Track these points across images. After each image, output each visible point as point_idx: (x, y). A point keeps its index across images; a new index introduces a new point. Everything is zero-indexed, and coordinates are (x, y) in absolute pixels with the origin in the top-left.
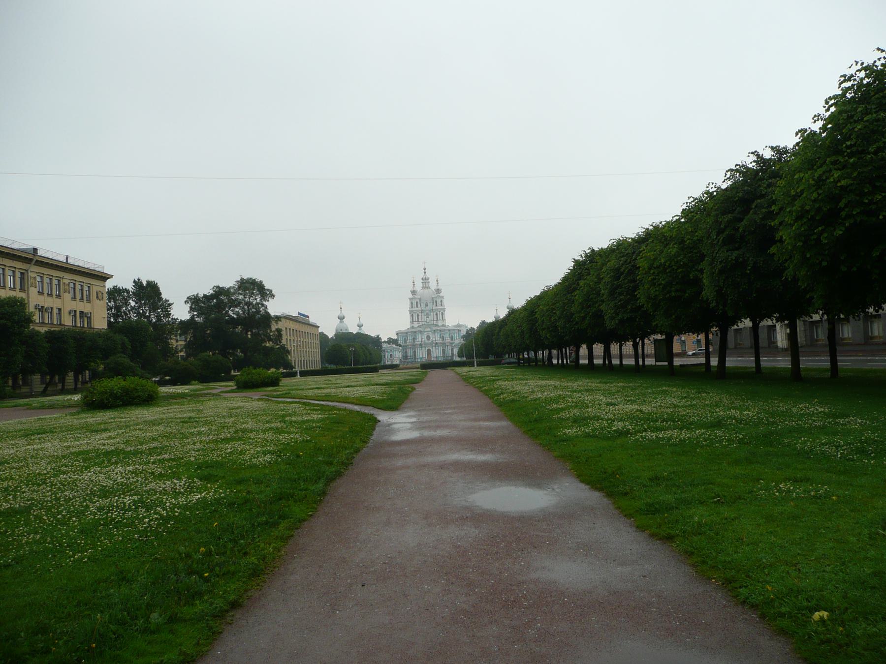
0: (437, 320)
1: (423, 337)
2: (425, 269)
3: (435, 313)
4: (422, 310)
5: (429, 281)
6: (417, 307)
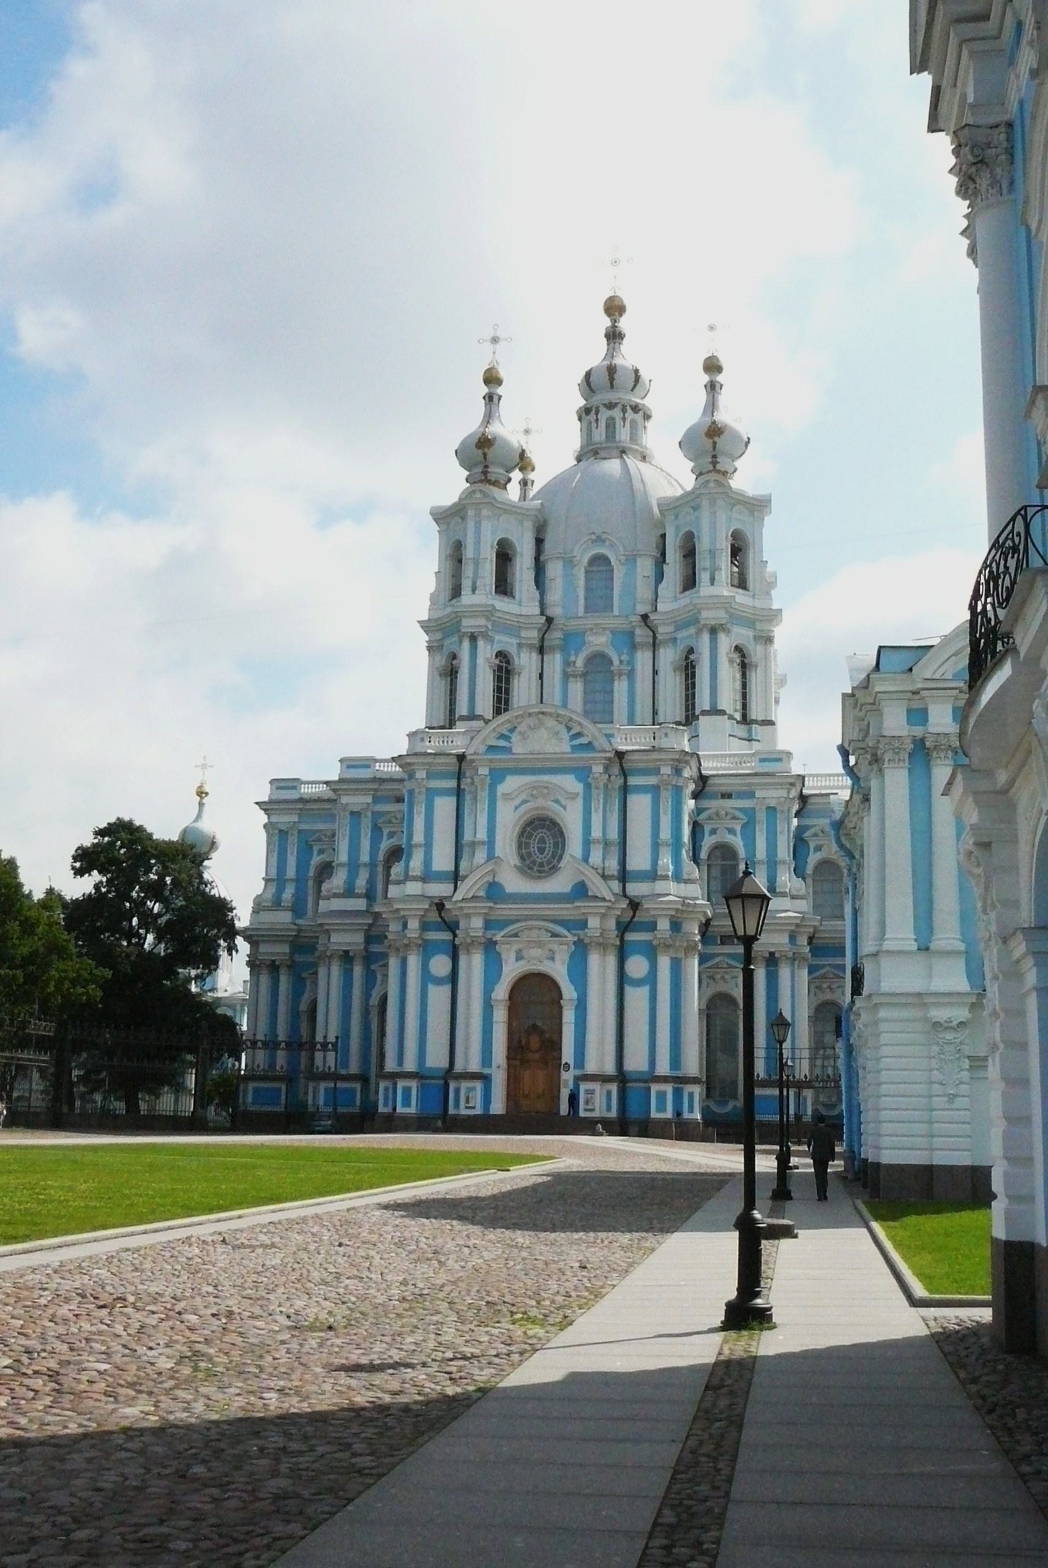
0: (690, 718)
1: (477, 829)
3: (668, 656)
4: (550, 620)
6: (503, 586)
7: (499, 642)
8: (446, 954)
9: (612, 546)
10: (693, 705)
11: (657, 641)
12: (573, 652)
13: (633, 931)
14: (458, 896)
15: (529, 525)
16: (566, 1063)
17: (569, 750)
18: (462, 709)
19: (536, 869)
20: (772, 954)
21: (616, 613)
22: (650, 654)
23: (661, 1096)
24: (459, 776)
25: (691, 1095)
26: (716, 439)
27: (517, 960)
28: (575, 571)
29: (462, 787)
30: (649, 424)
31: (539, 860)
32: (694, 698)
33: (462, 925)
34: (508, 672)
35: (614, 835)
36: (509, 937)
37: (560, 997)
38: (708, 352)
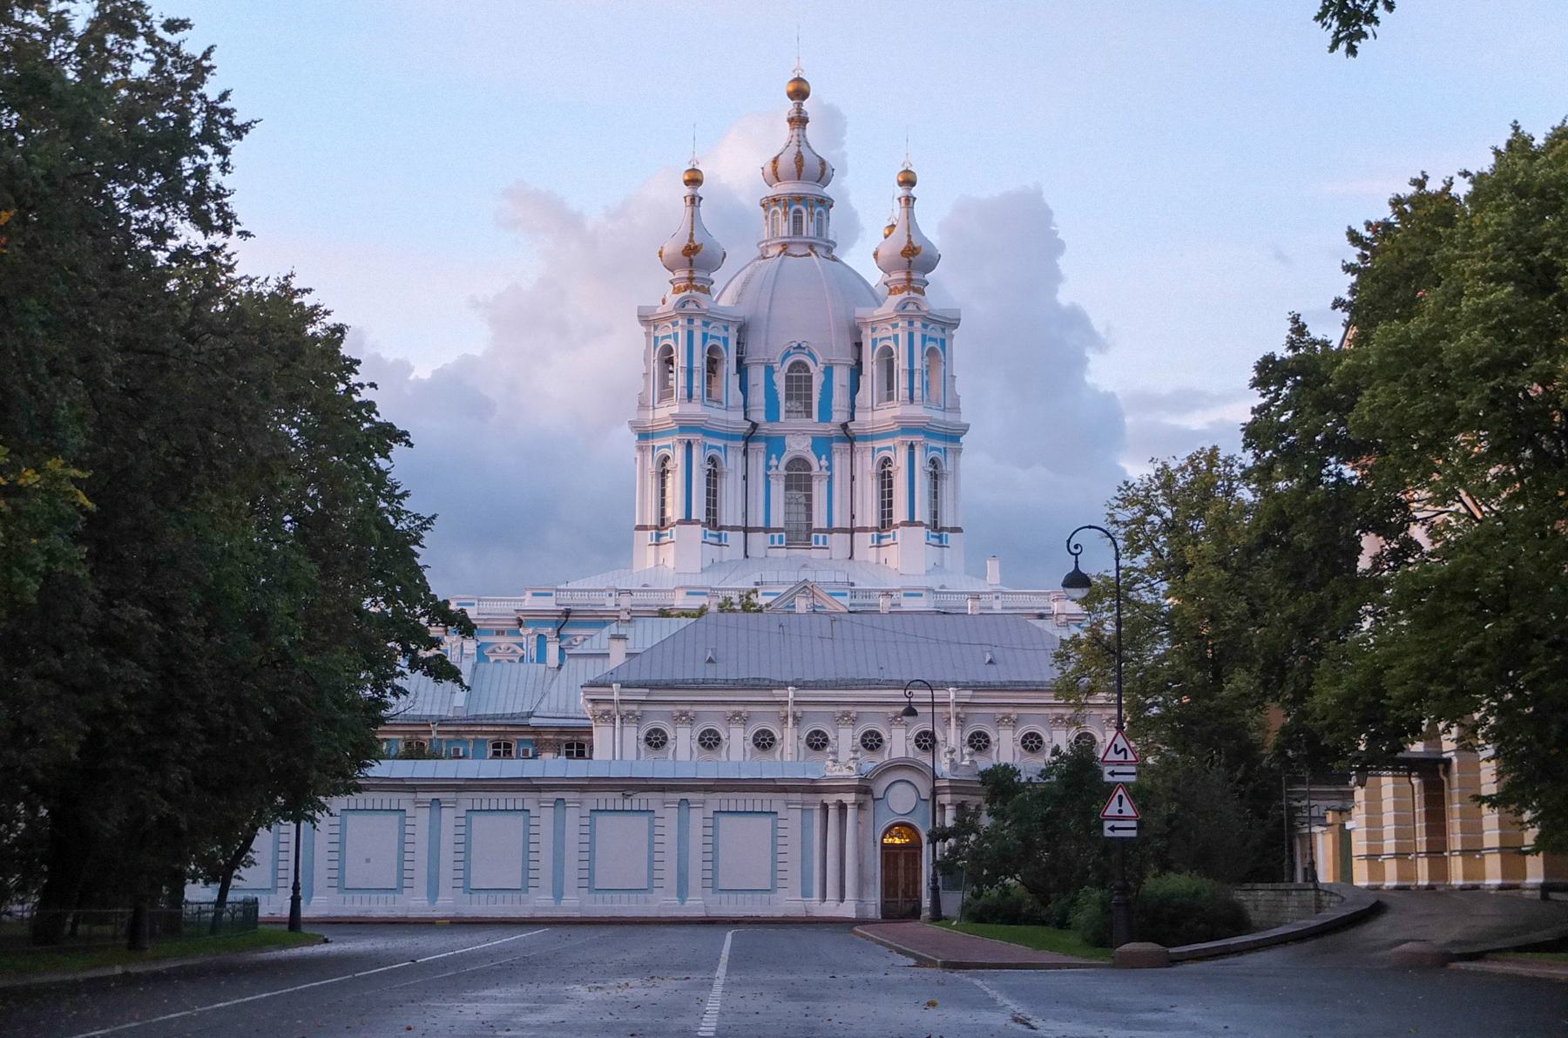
0: (886, 523)
2: (799, 92)
4: (755, 426)
5: (828, 191)
9: (811, 355)
10: (890, 514)
12: (774, 456)
15: (733, 331)
30: (831, 210)
32: (890, 504)
34: (715, 476)
38: (903, 165)
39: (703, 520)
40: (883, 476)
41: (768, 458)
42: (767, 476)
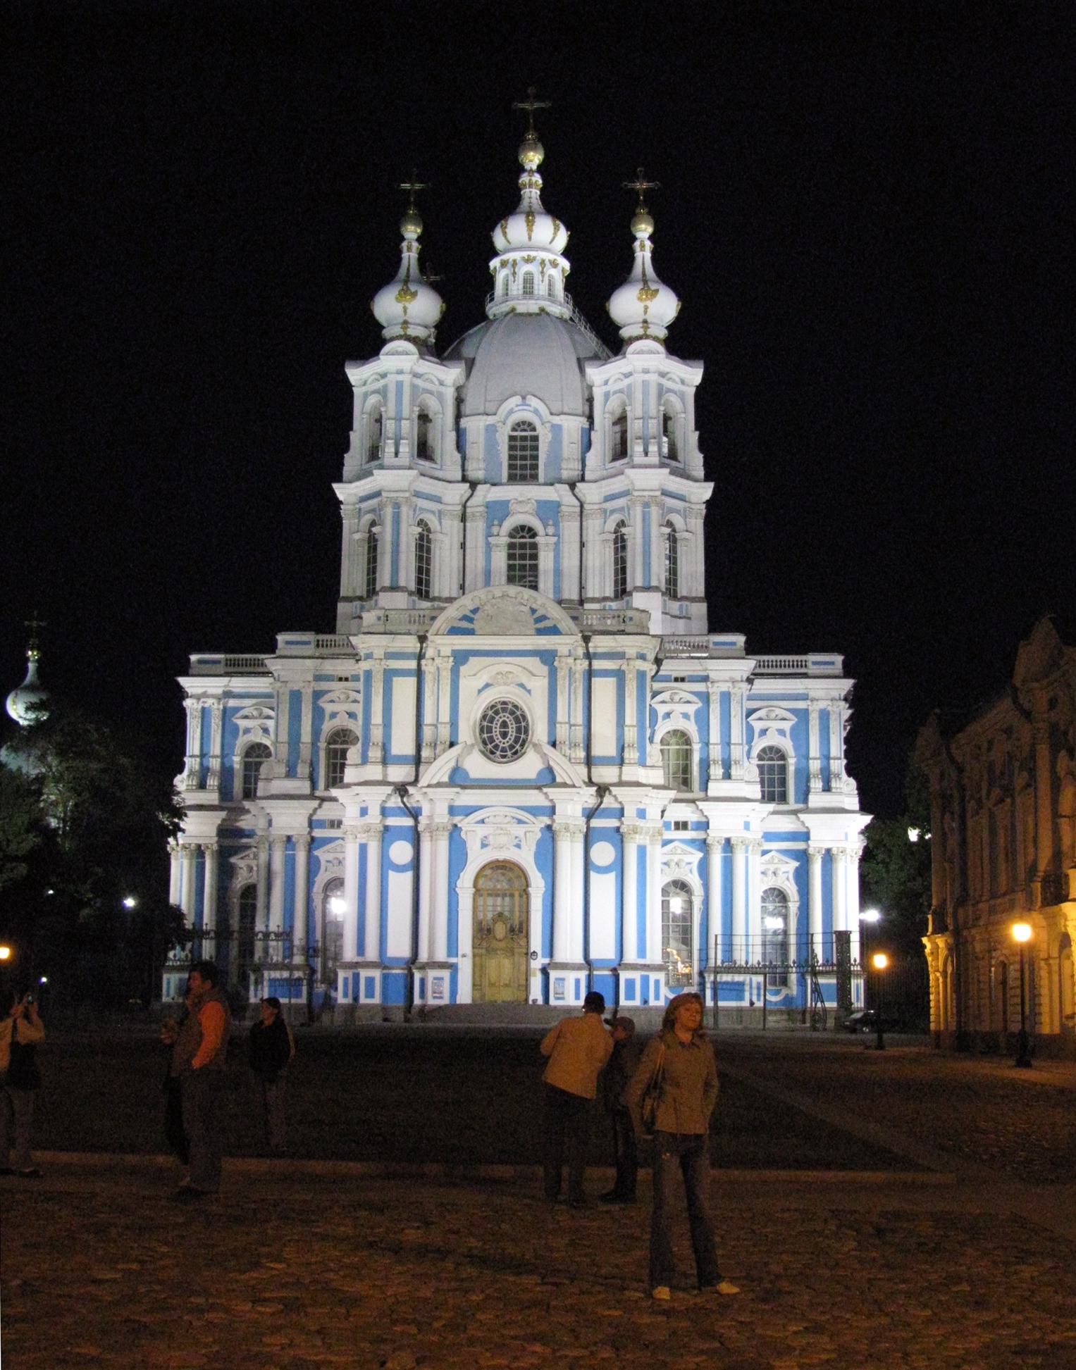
0: (622, 591)
6: (424, 450)
7: (420, 509)
8: (408, 841)
10: (624, 581)
11: (584, 514)
12: (496, 522)
13: (600, 817)
14: (423, 781)
16: (534, 952)
17: (533, 632)
18: (384, 579)
19: (498, 753)
20: (728, 841)
21: (541, 478)
22: (578, 524)
23: (630, 983)
24: (420, 656)
25: (657, 982)
26: (648, 303)
27: (482, 848)
28: (498, 435)
29: (423, 668)
31: (501, 745)
33: (426, 811)
34: (429, 541)
35: (579, 718)
36: (478, 822)
37: (527, 886)
39: (414, 590)
40: (616, 542)
41: (489, 526)
42: (488, 545)
